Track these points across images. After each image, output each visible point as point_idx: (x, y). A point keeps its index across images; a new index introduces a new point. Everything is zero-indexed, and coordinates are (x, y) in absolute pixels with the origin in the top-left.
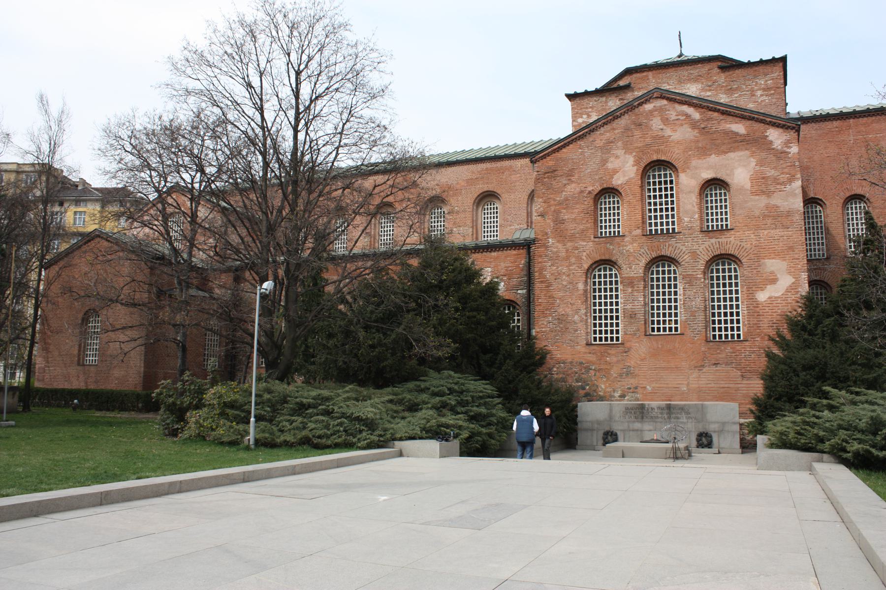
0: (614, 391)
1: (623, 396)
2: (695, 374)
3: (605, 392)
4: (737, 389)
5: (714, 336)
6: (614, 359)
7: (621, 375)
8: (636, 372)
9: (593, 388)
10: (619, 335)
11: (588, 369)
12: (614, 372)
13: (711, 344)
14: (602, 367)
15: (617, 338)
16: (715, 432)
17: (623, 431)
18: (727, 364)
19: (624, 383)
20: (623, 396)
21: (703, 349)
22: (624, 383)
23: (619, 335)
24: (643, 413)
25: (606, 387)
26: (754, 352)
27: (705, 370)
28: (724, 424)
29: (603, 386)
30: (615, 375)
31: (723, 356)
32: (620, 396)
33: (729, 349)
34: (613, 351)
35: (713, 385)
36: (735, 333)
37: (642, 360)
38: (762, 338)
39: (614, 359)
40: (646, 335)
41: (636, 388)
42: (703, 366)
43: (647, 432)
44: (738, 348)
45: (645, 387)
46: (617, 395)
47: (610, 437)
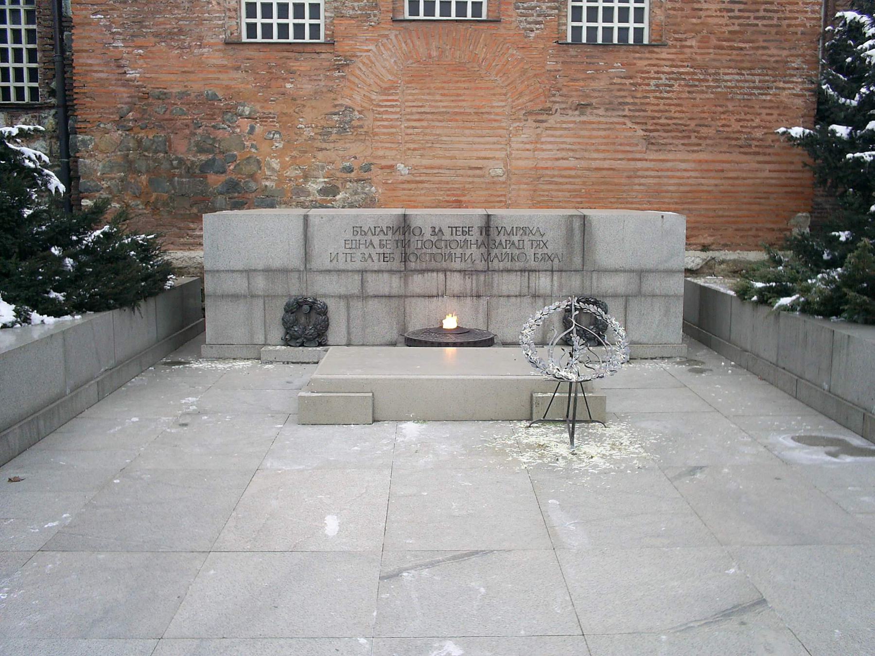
0: (306, 177)
1: (330, 191)
2: (528, 132)
3: (281, 180)
4: (633, 175)
5: (577, 31)
6: (308, 87)
7: (325, 133)
8: (368, 123)
9: (247, 169)
10: (321, 21)
11: (231, 112)
12: (307, 123)
13: (572, 51)
14: (274, 108)
15: (315, 29)
16: (615, 296)
17: (347, 298)
18: (610, 107)
19: (332, 155)
20: (330, 191)
21: (550, 64)
22: (332, 155)
23: (321, 21)
24: (405, 244)
25: (284, 167)
26: (679, 77)
27: (552, 121)
28: (641, 273)
29: (275, 164)
30: (309, 133)
31: (601, 84)
32: (320, 191)
33: (617, 68)
34: (302, 65)
35: (572, 163)
36: (631, 25)
37: (385, 91)
38: (704, 41)
39: (308, 87)
40: (394, 21)
41: (367, 168)
42: (548, 111)
43: (421, 302)
44: (641, 64)
45: (391, 167)
46: (314, 187)
47: (306, 325)
